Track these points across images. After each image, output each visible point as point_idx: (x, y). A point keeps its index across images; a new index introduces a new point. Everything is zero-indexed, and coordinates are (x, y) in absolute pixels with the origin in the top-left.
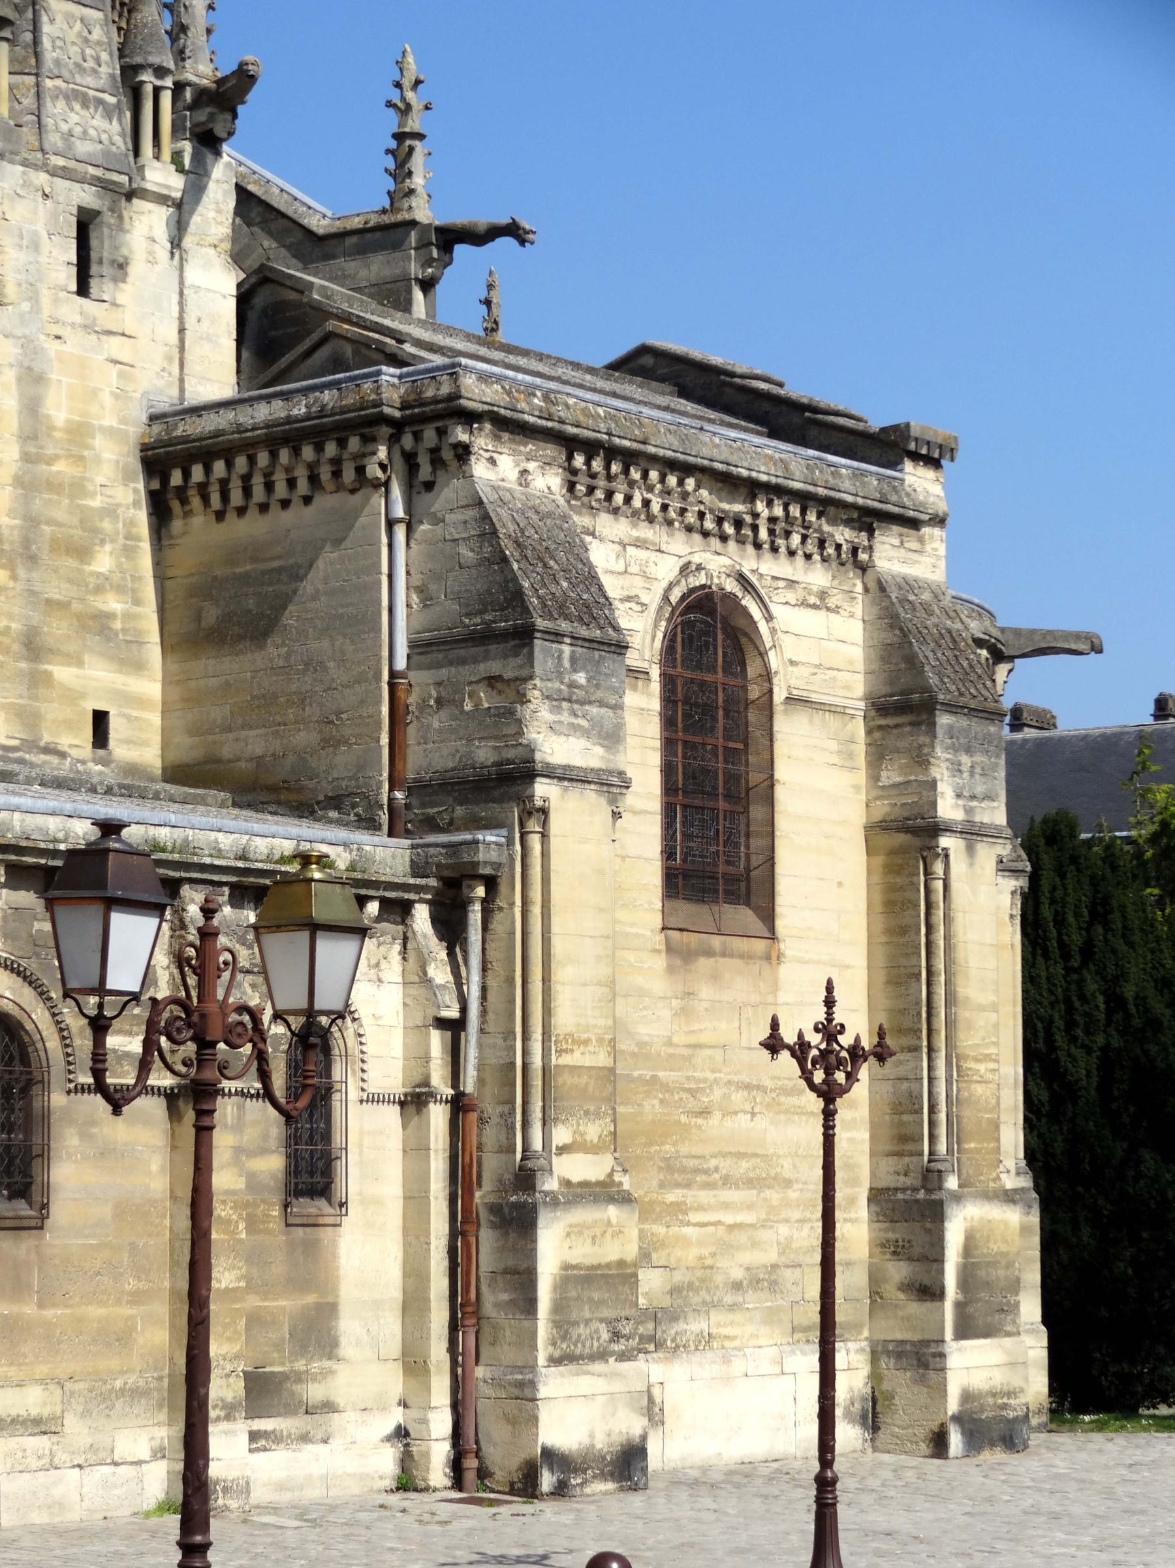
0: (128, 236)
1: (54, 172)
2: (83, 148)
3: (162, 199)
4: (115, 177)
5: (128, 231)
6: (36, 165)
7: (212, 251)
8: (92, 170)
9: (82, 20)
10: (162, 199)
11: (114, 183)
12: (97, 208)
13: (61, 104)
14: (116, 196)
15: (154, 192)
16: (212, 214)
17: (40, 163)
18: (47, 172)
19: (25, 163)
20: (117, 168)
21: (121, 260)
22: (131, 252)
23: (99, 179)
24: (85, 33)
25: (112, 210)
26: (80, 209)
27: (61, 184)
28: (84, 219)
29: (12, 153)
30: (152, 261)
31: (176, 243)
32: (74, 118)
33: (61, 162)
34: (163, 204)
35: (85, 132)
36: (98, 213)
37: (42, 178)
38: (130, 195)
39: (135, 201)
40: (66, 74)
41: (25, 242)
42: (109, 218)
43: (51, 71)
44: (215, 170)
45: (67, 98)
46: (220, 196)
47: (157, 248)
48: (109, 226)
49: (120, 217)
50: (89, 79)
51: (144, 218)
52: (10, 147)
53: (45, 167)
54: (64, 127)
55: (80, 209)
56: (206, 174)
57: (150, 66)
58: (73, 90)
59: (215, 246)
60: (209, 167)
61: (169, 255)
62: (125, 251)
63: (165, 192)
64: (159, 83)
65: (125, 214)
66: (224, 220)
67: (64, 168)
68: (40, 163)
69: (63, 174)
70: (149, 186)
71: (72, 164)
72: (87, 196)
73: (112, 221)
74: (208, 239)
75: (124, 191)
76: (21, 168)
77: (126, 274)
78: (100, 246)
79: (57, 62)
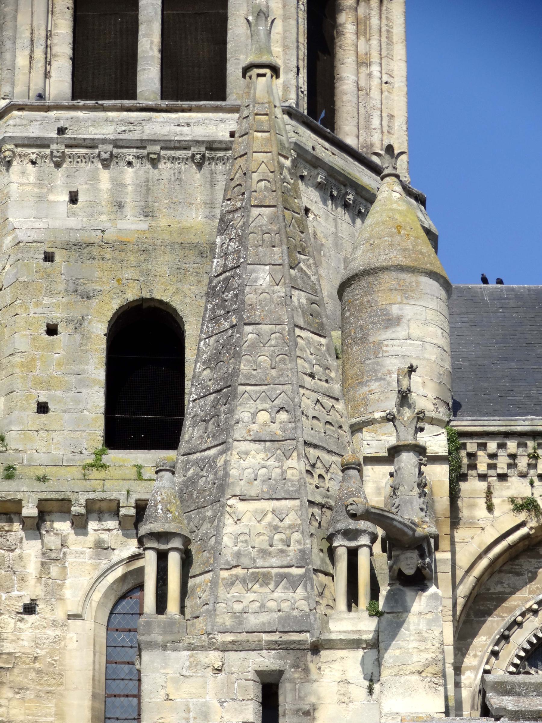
0: (315, 685)
1: (224, 648)
2: (253, 621)
3: (354, 644)
4: (295, 637)
5: (315, 681)
6: (203, 647)
7: (416, 677)
8: (265, 637)
9: (273, 512)
10: (354, 644)
11: (294, 642)
12: (278, 668)
13: (238, 588)
14: (300, 653)
15: (341, 640)
16: (413, 644)
17: (206, 644)
18: (217, 649)
19: (190, 648)
20: (295, 628)
21: (307, 708)
22: (319, 698)
23: (276, 642)
24: (277, 522)
25: (296, 666)
26: (259, 673)
27: (233, 657)
28: (268, 680)
29: (173, 642)
30: (345, 700)
31: (372, 679)
32: (251, 596)
33: (229, 638)
34: (358, 648)
35: (263, 606)
36: (281, 673)
37: (213, 657)
38: (316, 649)
39: (323, 653)
40: (245, 561)
41: (192, 715)
42: (291, 674)
43: (227, 563)
44: (415, 604)
45: (244, 581)
46: (423, 626)
47: (351, 688)
48: (292, 681)
49: (307, 671)
50: (273, 560)
51: (335, 666)
52: (169, 638)
53: (212, 646)
54: (238, 607)
55: (259, 673)
56: (406, 610)
57: (338, 532)
58: (253, 573)
59: (420, 673)
60: (409, 604)
61: (366, 691)
62: (312, 699)
63: (355, 637)
64: (353, 544)
65: (312, 666)
66: (429, 646)
67: (233, 642)
68: (206, 644)
69: (235, 647)
70: (333, 636)
71: (243, 637)
72: (268, 661)
73: (296, 675)
74: (409, 667)
75: (307, 647)
76: (189, 653)
77: (314, 719)
78: (286, 700)
79: (238, 555)
